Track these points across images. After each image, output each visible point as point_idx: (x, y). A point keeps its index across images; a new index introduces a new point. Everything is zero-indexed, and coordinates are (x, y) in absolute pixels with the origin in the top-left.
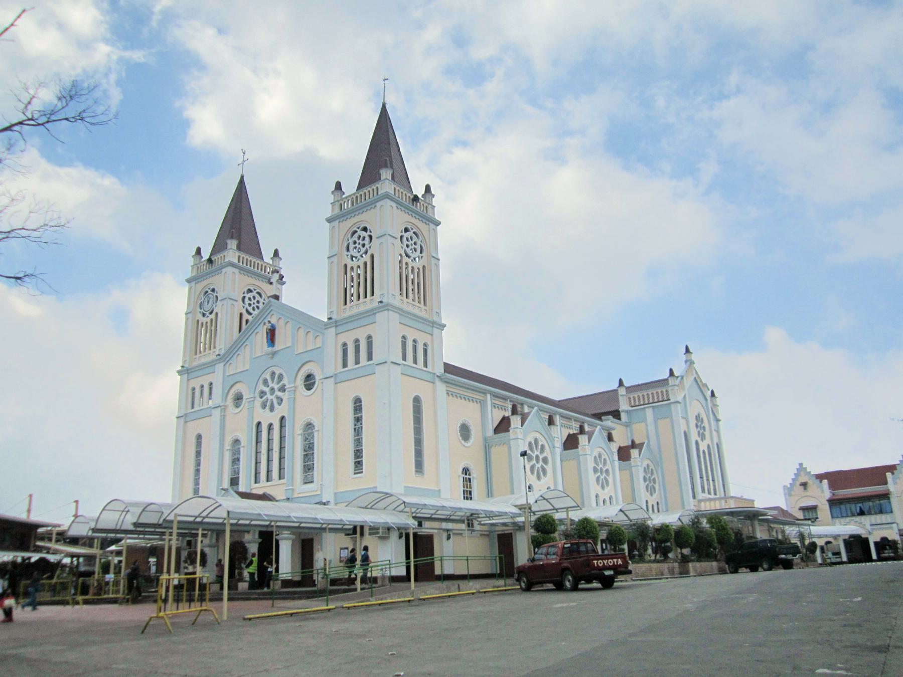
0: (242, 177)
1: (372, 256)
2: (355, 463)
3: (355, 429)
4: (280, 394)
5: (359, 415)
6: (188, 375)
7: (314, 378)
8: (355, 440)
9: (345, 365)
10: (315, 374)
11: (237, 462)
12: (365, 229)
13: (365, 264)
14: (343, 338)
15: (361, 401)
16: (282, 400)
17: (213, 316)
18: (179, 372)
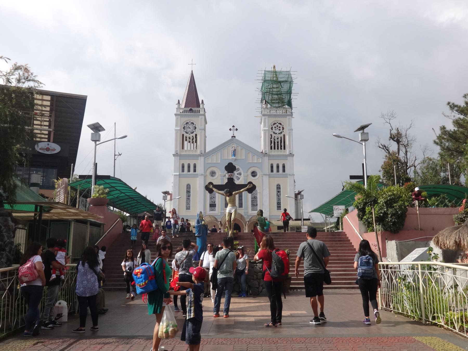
0: (192, 71)
1: (284, 135)
2: (277, 206)
3: (277, 195)
4: (238, 176)
5: (279, 190)
6: (180, 157)
7: (256, 173)
8: (277, 199)
9: (272, 171)
10: (256, 171)
11: (213, 198)
12: (280, 124)
13: (281, 138)
14: (271, 162)
15: (280, 186)
16: (239, 178)
17: (194, 135)
18: (173, 155)
